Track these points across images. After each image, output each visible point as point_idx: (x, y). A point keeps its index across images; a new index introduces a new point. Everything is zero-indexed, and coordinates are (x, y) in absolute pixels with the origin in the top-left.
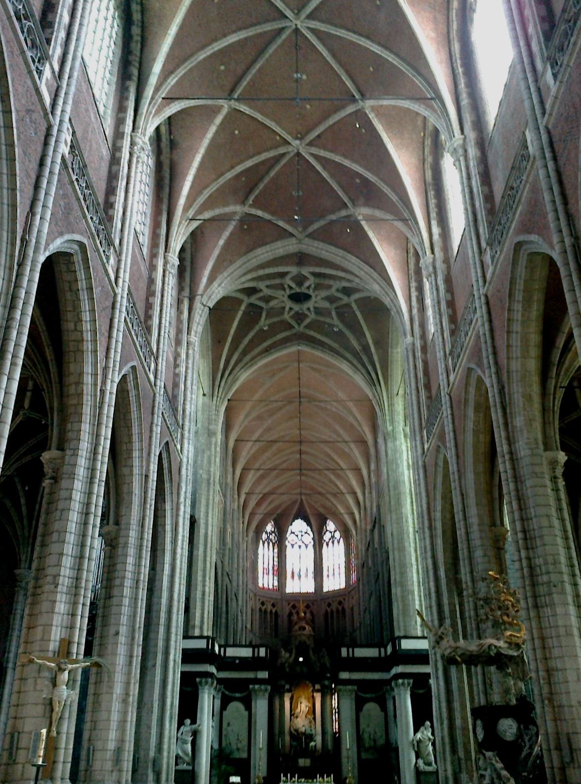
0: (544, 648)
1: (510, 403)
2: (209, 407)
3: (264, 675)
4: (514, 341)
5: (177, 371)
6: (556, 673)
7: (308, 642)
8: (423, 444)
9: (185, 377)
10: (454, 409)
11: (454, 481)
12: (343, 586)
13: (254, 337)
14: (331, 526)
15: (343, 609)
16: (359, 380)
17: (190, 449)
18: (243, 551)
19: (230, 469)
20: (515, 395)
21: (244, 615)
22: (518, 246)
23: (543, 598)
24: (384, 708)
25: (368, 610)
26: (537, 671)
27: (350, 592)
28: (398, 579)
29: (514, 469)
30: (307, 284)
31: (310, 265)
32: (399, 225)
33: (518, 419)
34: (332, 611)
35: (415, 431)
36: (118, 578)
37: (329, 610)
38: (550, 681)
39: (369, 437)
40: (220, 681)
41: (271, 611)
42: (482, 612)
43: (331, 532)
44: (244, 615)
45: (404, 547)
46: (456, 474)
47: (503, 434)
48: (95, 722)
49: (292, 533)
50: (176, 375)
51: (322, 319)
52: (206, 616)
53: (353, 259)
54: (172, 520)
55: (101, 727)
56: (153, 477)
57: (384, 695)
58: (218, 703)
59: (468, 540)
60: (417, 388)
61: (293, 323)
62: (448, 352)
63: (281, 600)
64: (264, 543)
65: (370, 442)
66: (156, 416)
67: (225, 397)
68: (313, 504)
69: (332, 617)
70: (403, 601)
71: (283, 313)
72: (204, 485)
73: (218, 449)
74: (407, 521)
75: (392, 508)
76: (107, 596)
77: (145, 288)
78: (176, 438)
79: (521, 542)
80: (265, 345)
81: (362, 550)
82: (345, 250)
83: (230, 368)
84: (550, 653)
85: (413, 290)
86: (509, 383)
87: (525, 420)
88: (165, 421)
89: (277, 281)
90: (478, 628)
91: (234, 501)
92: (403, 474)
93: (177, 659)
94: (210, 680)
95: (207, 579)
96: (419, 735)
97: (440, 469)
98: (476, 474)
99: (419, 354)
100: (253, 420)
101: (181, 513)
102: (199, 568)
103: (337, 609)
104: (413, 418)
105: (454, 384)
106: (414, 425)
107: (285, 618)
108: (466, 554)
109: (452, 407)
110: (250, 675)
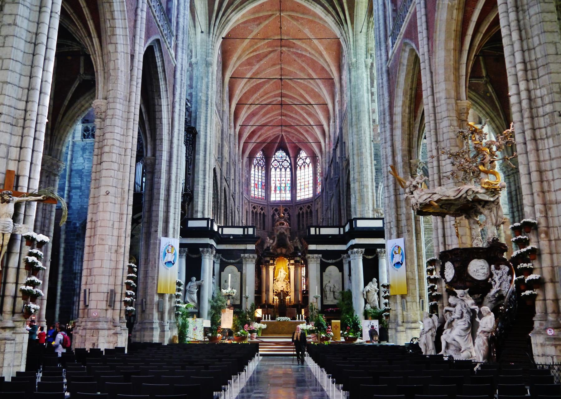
0: (542, 181)
2: (207, 43)
3: (252, 247)
6: (554, 207)
7: (286, 233)
8: (387, 52)
11: (424, 62)
12: (311, 196)
14: (303, 154)
15: (311, 212)
16: (330, 21)
17: (184, 57)
21: (241, 213)
24: (341, 270)
26: (533, 206)
27: (316, 200)
28: (356, 177)
34: (303, 212)
35: (380, 42)
37: (301, 212)
38: (547, 214)
40: (218, 251)
41: (260, 213)
44: (241, 213)
45: (362, 153)
48: (90, 269)
52: (206, 204)
54: (168, 114)
55: (95, 274)
56: (139, 57)
57: (342, 260)
58: (217, 266)
63: (268, 205)
64: (255, 167)
65: (336, 79)
68: (290, 138)
69: (303, 217)
72: (203, 105)
74: (365, 133)
75: (353, 123)
76: (99, 162)
78: (170, 43)
83: (223, 9)
84: (549, 185)
91: (230, 128)
92: (363, 96)
93: (176, 227)
94: (210, 249)
95: (207, 177)
96: (368, 288)
98: (447, 50)
101: (177, 110)
102: (200, 169)
103: (307, 212)
104: (379, 31)
106: (380, 39)
107: (270, 217)
110: (242, 247)
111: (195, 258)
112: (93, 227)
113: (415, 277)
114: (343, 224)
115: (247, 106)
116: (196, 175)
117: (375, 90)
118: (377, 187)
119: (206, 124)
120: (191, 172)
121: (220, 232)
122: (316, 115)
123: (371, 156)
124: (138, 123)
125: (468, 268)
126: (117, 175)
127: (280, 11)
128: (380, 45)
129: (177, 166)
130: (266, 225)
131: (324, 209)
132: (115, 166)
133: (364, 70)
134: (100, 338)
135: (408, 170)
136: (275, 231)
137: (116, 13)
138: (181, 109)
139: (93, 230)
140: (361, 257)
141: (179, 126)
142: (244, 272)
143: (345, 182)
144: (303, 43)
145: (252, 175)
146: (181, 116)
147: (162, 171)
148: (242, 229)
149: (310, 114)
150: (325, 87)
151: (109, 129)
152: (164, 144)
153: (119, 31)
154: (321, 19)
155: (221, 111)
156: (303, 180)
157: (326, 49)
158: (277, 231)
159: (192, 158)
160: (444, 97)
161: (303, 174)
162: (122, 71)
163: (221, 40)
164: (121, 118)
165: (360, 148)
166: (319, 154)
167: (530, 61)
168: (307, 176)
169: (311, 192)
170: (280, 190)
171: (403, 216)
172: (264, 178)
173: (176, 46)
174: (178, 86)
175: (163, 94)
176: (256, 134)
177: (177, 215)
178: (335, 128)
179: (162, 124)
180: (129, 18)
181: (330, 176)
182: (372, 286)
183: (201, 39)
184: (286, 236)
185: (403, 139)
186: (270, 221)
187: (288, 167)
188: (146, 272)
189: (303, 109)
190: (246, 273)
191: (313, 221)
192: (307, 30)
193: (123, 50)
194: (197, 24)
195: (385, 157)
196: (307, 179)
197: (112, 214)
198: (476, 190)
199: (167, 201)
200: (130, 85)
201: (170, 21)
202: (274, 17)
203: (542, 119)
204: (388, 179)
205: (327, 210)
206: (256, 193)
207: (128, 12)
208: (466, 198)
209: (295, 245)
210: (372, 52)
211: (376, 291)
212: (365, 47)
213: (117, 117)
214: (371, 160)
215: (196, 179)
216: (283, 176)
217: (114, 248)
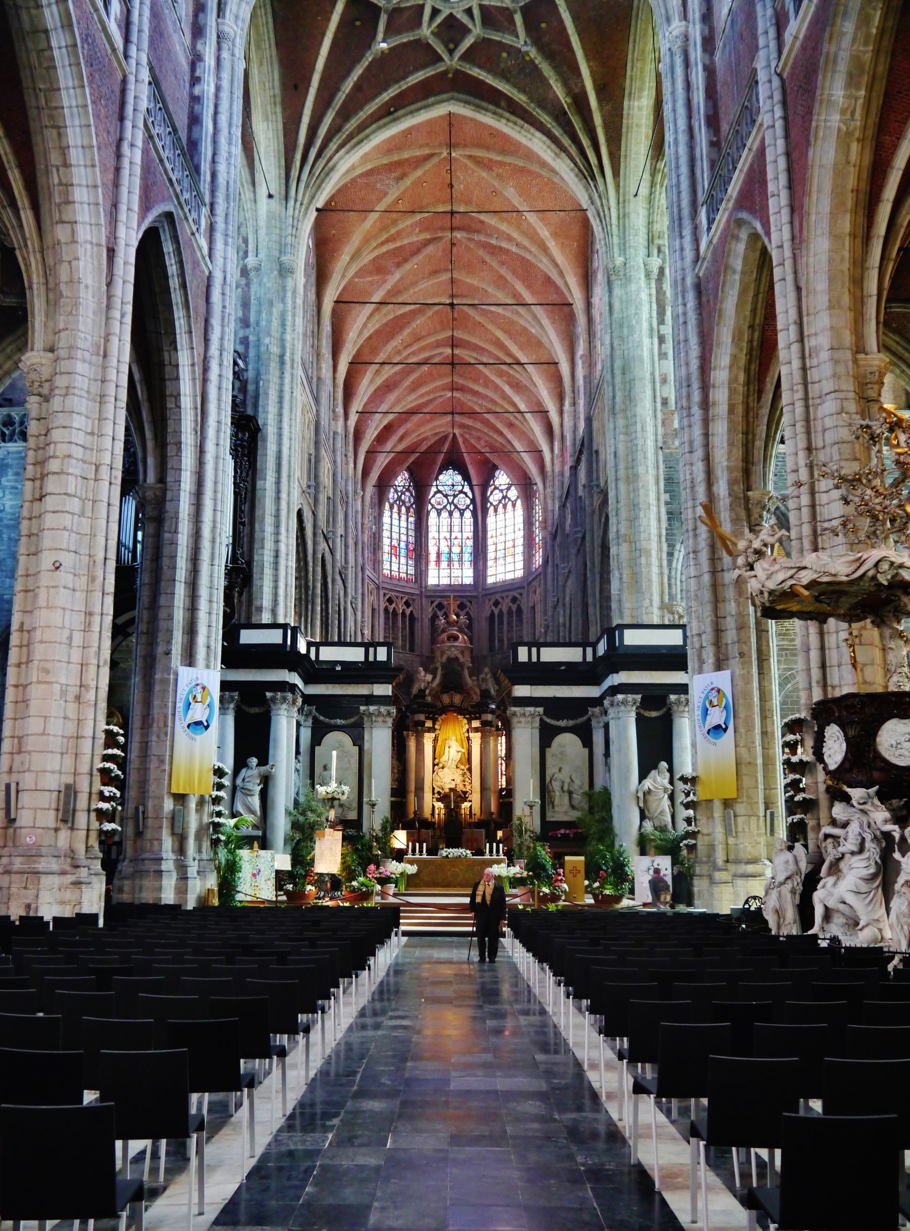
2: (280, 221)
5: (197, 91)
7: (461, 659)
8: (696, 241)
9: (216, 106)
12: (520, 573)
13: (361, 77)
14: (502, 479)
15: (519, 610)
16: (564, 169)
17: (229, 255)
21: (359, 613)
24: (587, 742)
25: (560, 604)
27: (530, 583)
28: (623, 531)
34: (501, 611)
35: (680, 219)
36: (54, 457)
37: (496, 611)
39: (577, 297)
40: (308, 699)
41: (403, 613)
43: (502, 491)
44: (359, 613)
45: (636, 476)
48: (20, 738)
49: (439, 491)
50: (195, 100)
51: (496, 37)
52: (281, 592)
55: (29, 748)
57: (589, 720)
58: (306, 734)
61: (440, 49)
63: (421, 595)
64: (391, 507)
66: (128, 124)
67: (310, 202)
68: (473, 441)
69: (501, 623)
71: (420, 24)
72: (274, 366)
74: (643, 430)
76: (37, 496)
78: (197, 222)
80: (386, 96)
81: (553, 511)
83: (318, 143)
91: (335, 418)
92: (640, 345)
94: (289, 695)
95: (283, 530)
99: (697, 54)
103: (510, 612)
104: (679, 193)
106: (680, 210)
107: (426, 622)
110: (362, 690)
111: (256, 714)
112: (25, 643)
113: (756, 759)
114: (592, 639)
115: (374, 368)
116: (257, 526)
117: (667, 330)
118: (670, 554)
119: (281, 408)
120: (246, 520)
121: (313, 656)
122: (532, 388)
123: (657, 483)
124: (124, 405)
125: (878, 739)
126: (79, 524)
127: (450, 146)
128: (680, 225)
129: (215, 505)
130: (418, 640)
131: (550, 604)
132: (74, 505)
133: (643, 282)
134: (42, 894)
135: (743, 514)
136: (438, 653)
137: (72, 151)
138: (224, 374)
139: (24, 649)
140: (633, 715)
141: (219, 414)
142: (366, 746)
143: (597, 542)
144: (502, 220)
145: (386, 527)
146: (224, 391)
147: (181, 515)
148: (362, 650)
149: (517, 386)
150: (553, 323)
151: (60, 420)
152: (184, 454)
153: (80, 194)
154: (544, 164)
155: (315, 379)
156: (502, 539)
157: (555, 235)
158: (443, 653)
159: (249, 488)
160: (827, 346)
161: (501, 524)
162: (87, 287)
163: (315, 214)
164: (85, 395)
165: (632, 464)
166: (538, 480)
168: (510, 529)
169: (520, 565)
170: (450, 560)
171: (729, 619)
172: (412, 533)
173: (212, 228)
174: (215, 322)
175: (182, 339)
177: (214, 617)
178: (575, 418)
179: (180, 407)
180: (102, 164)
181: (564, 529)
182: (659, 779)
183: (269, 212)
184: (461, 665)
185: (731, 444)
186: (427, 632)
187: (468, 507)
188: (145, 747)
189: (501, 374)
190: (371, 749)
191: (525, 632)
192: (512, 190)
193: (89, 238)
194: (259, 177)
195: (688, 484)
196: (510, 537)
197: (67, 612)
198: (898, 560)
200: (107, 318)
201: (197, 169)
202: (435, 160)
204: (695, 536)
205: (555, 607)
206: (395, 567)
207: (99, 148)
208: (874, 578)
209: (484, 687)
210: (661, 242)
211: (665, 790)
212: (645, 230)
213: (76, 391)
214: (658, 493)
215: (257, 534)
216: (456, 529)
217: (73, 691)
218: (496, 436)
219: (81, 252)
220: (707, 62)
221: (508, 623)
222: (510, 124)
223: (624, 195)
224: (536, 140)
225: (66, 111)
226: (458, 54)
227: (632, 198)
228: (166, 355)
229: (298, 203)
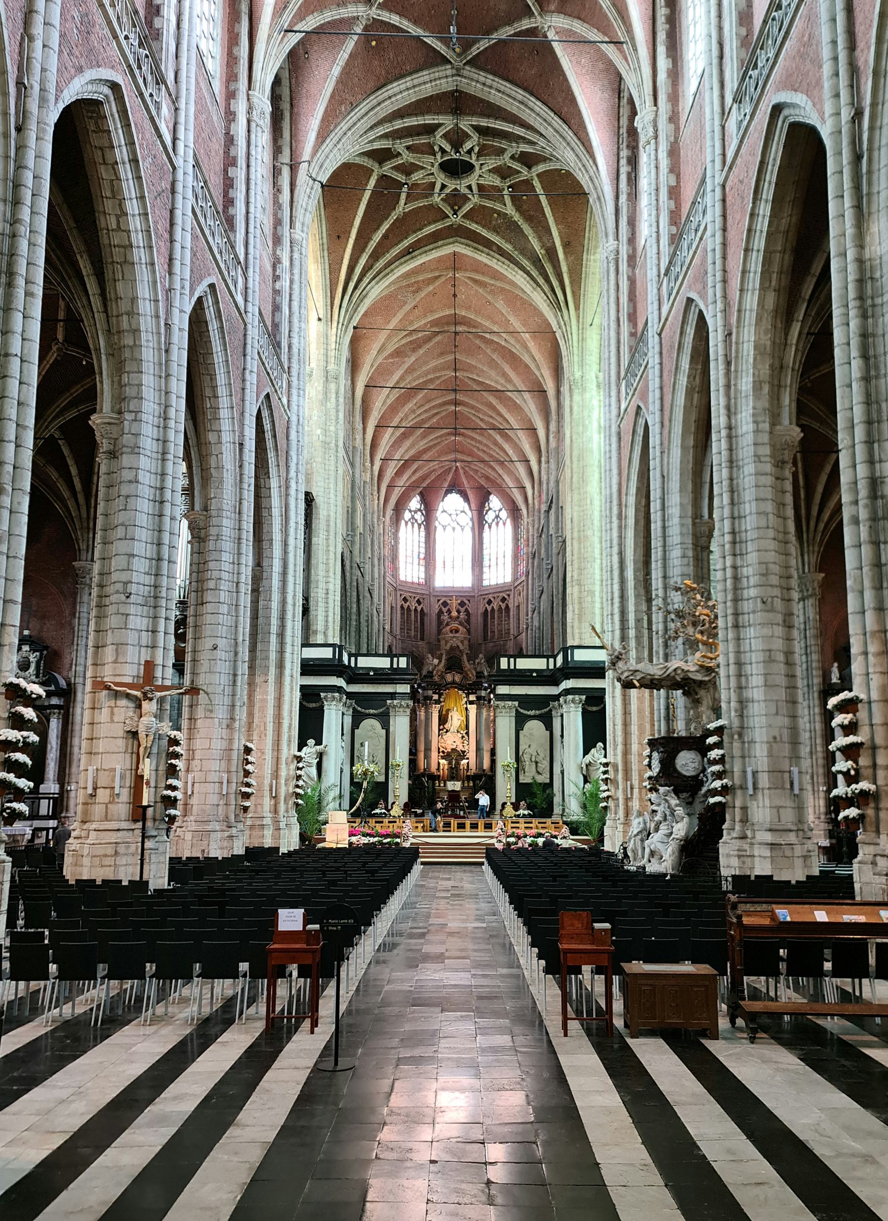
1: (737, 357)
4: (753, 265)
7: (461, 647)
10: (664, 356)
12: (508, 579)
13: (387, 230)
14: (495, 502)
15: (507, 607)
16: (539, 299)
18: (380, 534)
19: (359, 426)
20: (745, 345)
22: (777, 109)
23: (746, 616)
27: (516, 587)
28: (576, 577)
29: (730, 450)
30: (468, 145)
31: (473, 114)
32: (610, 50)
33: (744, 380)
35: (609, 383)
37: (489, 608)
41: (416, 610)
42: (672, 626)
44: (381, 615)
46: (658, 448)
47: (722, 401)
49: (444, 511)
51: (489, 204)
52: (330, 619)
53: (538, 106)
54: (281, 500)
56: (250, 446)
59: (664, 537)
60: (618, 319)
61: (448, 211)
62: (663, 271)
64: (406, 523)
69: (493, 617)
70: (580, 603)
73: (341, 400)
77: (222, 152)
79: (727, 546)
80: (406, 243)
82: (525, 89)
85: (623, 162)
86: (738, 327)
87: (754, 382)
88: (263, 364)
89: (423, 140)
90: (666, 646)
97: (639, 439)
98: (684, 447)
99: (624, 267)
100: (391, 355)
101: (292, 492)
103: (500, 608)
104: (610, 364)
105: (666, 319)
106: (609, 377)
107: (434, 617)
108: (660, 554)
109: (661, 353)
111: (311, 709)
122: (517, 441)
128: (609, 387)
129: (295, 580)
132: (224, 609)
136: (443, 642)
146: (299, 501)
155: (351, 447)
158: (447, 642)
164: (228, 539)
167: (740, 532)
172: (423, 545)
175: (273, 471)
176: (409, 467)
181: (540, 554)
186: (434, 624)
198: (686, 668)
199: (281, 635)
200: (241, 489)
202: (443, 279)
203: (746, 603)
209: (478, 670)
213: (224, 538)
218: (490, 471)
219: (224, 448)
220: (630, 274)
221: (499, 617)
222: (499, 263)
223: (583, 324)
224: (518, 277)
225: (216, 366)
226: (461, 213)
227: (588, 326)
228: (262, 481)
229: (340, 325)
